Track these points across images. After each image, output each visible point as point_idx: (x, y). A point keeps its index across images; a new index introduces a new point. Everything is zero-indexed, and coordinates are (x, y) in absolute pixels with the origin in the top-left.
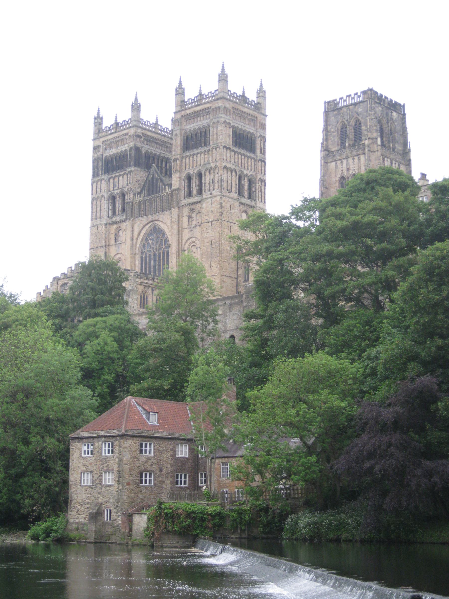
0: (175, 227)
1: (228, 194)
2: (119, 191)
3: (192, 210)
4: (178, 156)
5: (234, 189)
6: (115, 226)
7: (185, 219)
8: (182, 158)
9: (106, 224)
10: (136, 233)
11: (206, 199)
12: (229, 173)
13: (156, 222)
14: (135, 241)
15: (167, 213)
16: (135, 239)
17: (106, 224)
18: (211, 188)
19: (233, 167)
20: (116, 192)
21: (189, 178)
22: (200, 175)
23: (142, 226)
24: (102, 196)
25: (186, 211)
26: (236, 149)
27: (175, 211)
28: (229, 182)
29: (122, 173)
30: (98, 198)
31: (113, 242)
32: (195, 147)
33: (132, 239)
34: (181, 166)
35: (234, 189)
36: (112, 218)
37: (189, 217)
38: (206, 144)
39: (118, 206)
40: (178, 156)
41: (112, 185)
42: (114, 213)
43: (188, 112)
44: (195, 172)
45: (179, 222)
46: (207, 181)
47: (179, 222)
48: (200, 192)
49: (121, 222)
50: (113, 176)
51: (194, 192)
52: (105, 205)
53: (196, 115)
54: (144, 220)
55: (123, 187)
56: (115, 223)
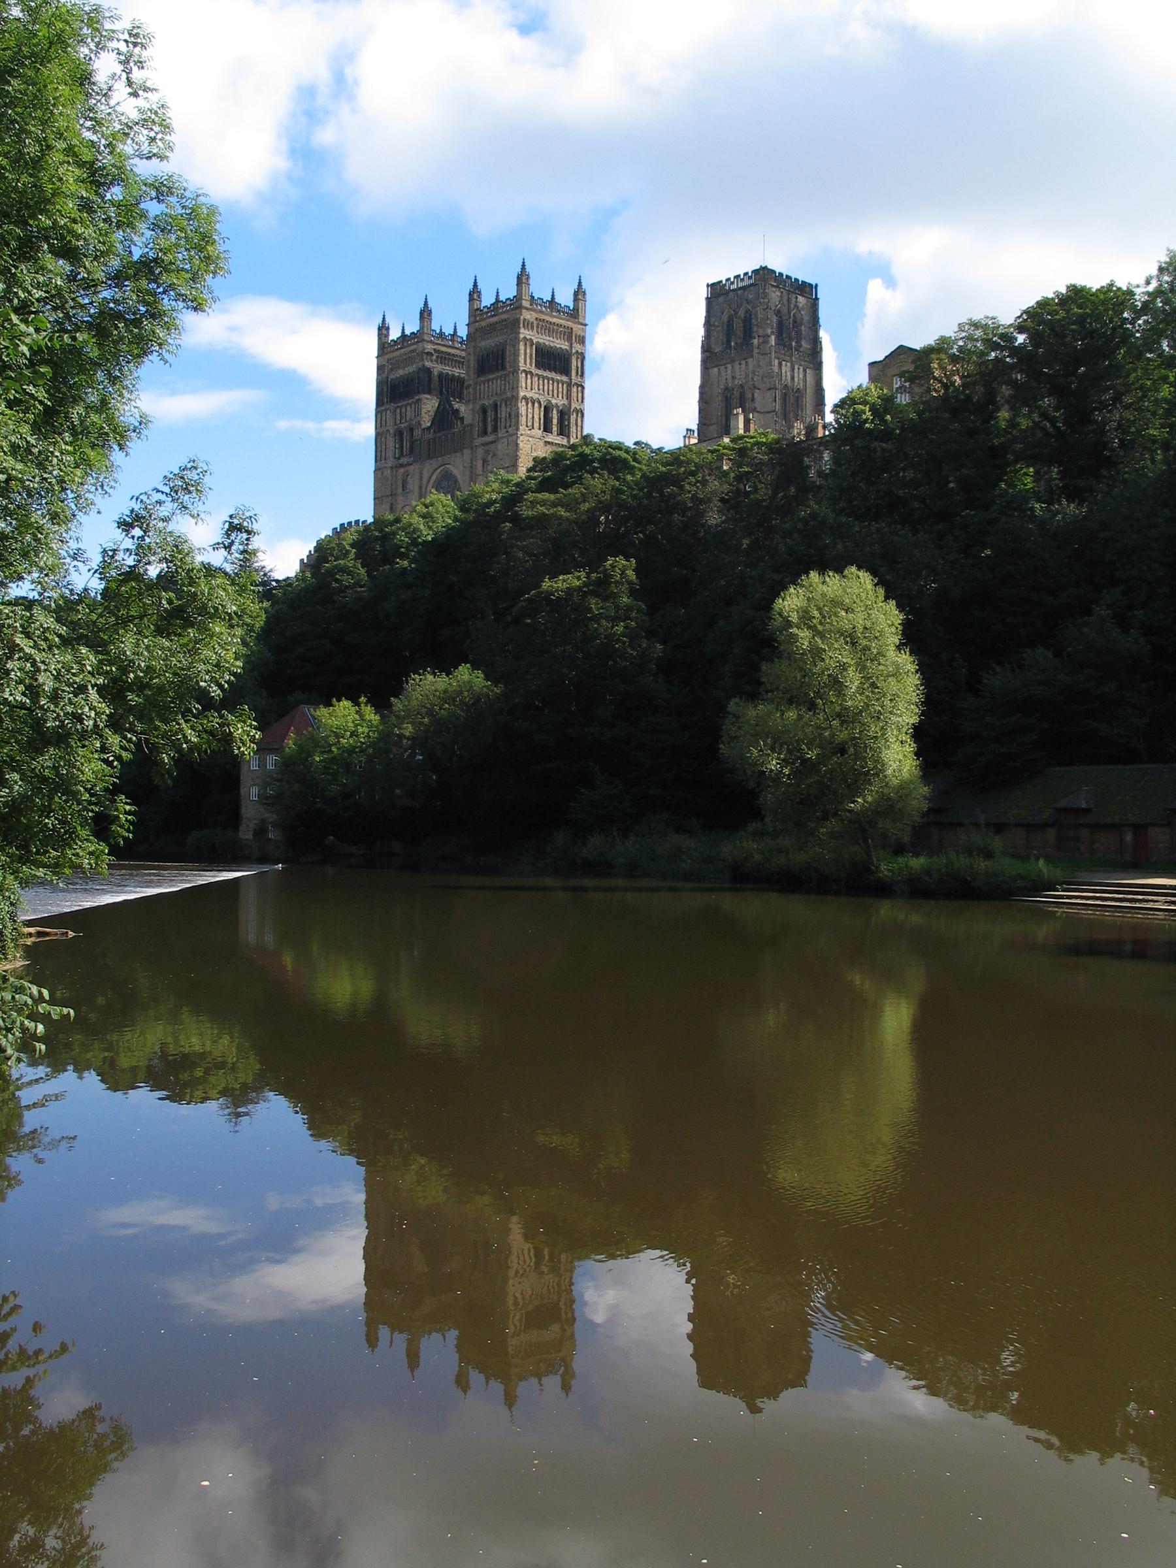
0: (467, 473)
1: (529, 432)
2: (407, 424)
3: (487, 452)
4: (471, 382)
5: (536, 425)
6: (402, 470)
7: (479, 463)
8: (476, 384)
9: (392, 468)
10: (425, 480)
11: (502, 438)
12: (530, 405)
13: (447, 466)
14: (424, 490)
15: (458, 454)
16: (424, 486)
17: (392, 468)
18: (508, 424)
19: (536, 396)
20: (403, 425)
21: (484, 411)
22: (495, 407)
23: (432, 470)
24: (388, 431)
25: (480, 452)
26: (540, 372)
27: (467, 452)
28: (530, 416)
29: (410, 401)
30: (383, 432)
31: (400, 490)
32: (491, 371)
33: (420, 488)
34: (475, 394)
35: (536, 425)
36: (399, 459)
37: (485, 461)
38: (503, 368)
39: (406, 445)
40: (471, 382)
41: (398, 417)
42: (401, 455)
43: (483, 324)
44: (491, 402)
45: (471, 467)
46: (503, 416)
47: (471, 467)
48: (495, 430)
49: (409, 464)
50: (400, 404)
51: (489, 429)
52: (391, 442)
53: (492, 328)
54: (434, 463)
55: (411, 420)
56: (402, 466)
